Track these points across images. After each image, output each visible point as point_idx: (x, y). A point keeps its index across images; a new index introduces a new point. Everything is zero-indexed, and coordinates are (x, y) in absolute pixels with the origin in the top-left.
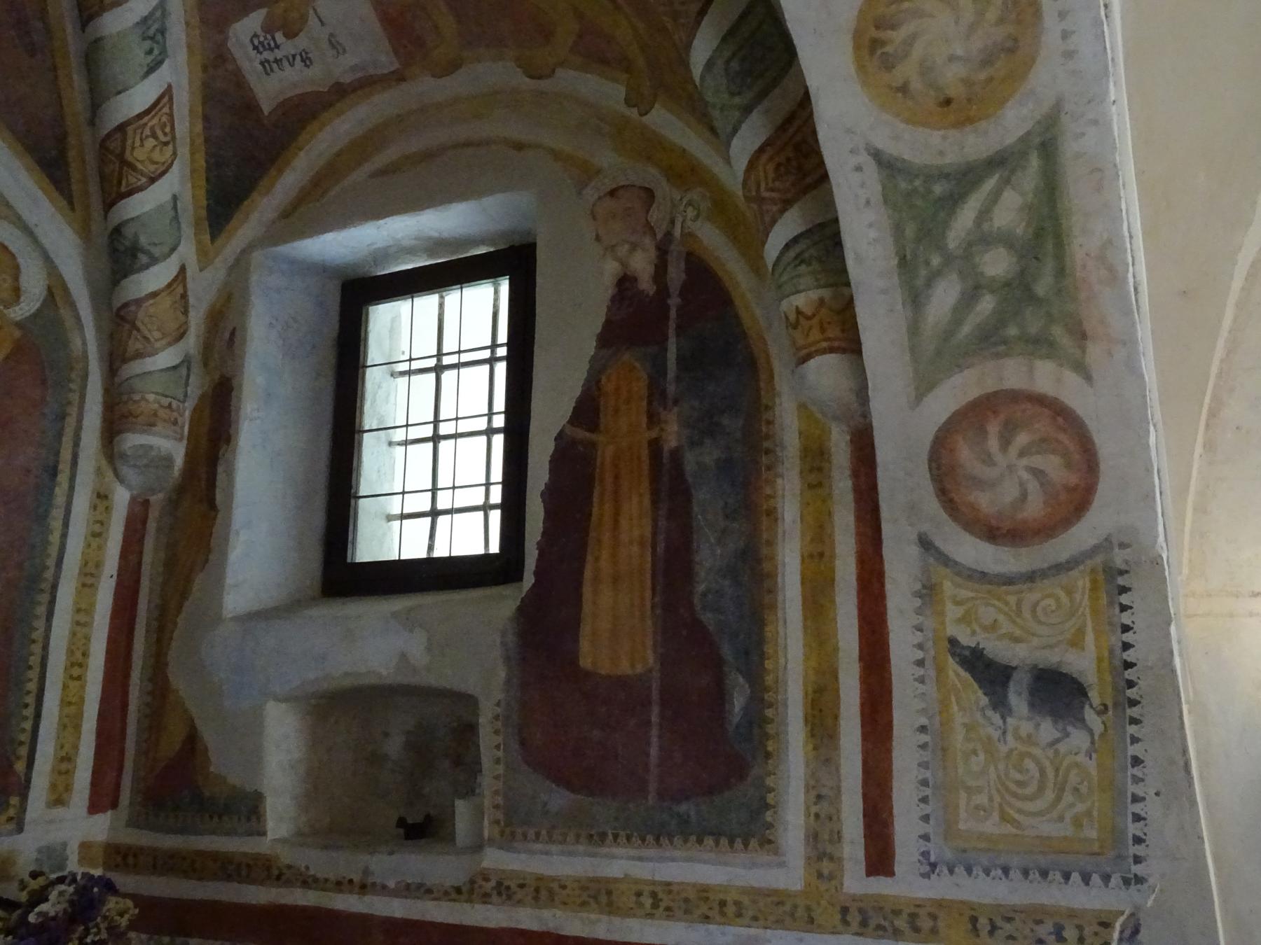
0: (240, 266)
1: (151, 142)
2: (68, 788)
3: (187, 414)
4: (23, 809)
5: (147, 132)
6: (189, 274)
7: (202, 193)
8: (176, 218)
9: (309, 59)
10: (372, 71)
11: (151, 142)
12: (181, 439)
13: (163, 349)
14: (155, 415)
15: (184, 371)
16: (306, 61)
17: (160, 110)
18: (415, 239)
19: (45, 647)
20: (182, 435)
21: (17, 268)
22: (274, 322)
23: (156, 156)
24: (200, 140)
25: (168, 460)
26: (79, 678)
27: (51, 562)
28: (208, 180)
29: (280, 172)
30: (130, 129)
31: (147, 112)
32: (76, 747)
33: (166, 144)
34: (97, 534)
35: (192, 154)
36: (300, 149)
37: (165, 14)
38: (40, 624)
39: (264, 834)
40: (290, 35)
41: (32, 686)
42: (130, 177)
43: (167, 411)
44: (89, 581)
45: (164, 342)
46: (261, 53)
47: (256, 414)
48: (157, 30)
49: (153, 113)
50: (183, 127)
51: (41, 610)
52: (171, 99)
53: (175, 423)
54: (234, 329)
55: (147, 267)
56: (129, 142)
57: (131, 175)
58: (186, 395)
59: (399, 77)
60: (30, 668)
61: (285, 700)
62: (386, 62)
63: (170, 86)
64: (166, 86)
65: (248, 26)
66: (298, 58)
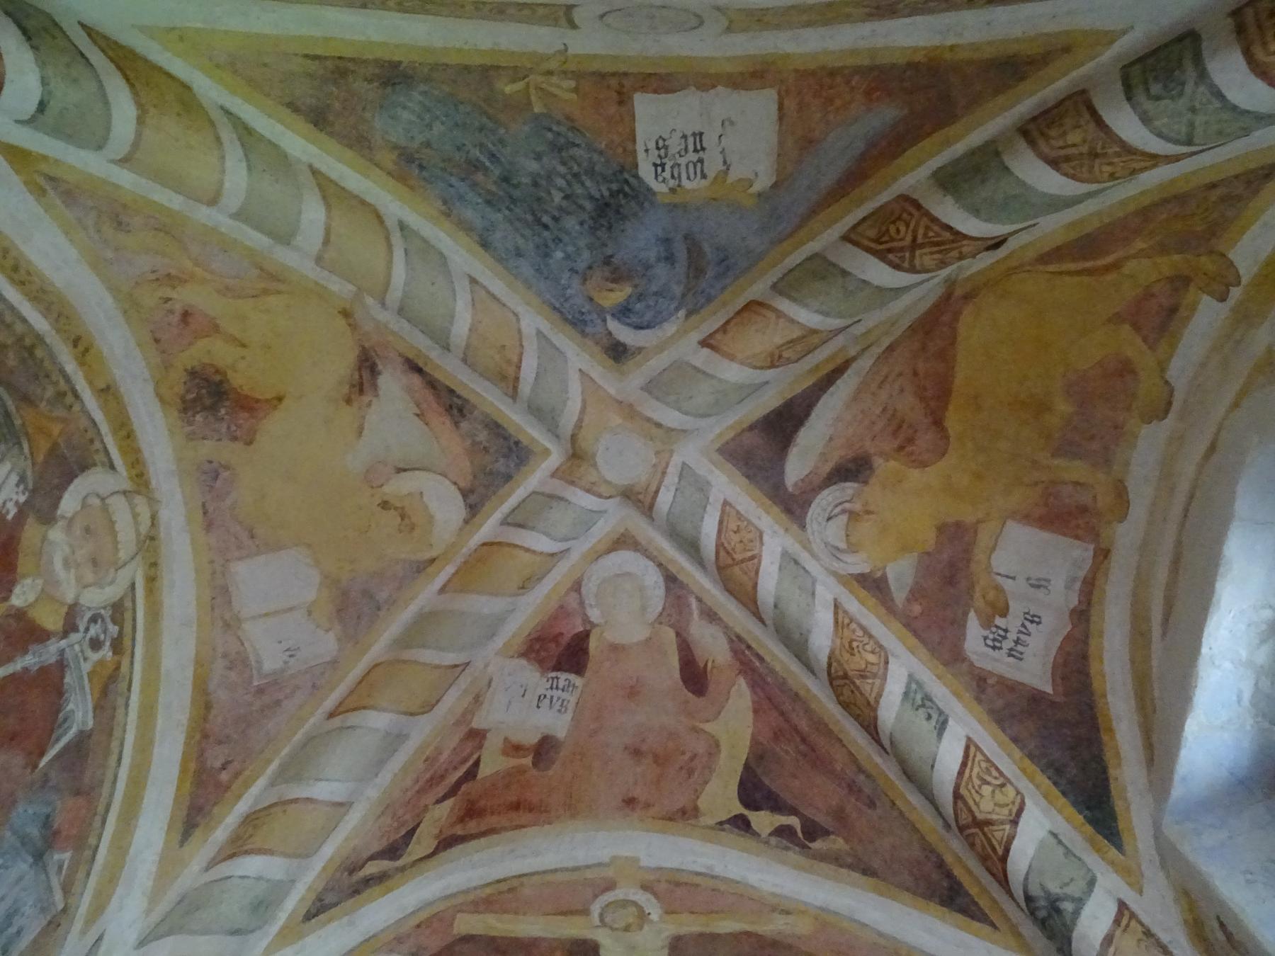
0: (1168, 856)
1: (987, 790)
5: (977, 782)
6: (1134, 906)
7: (1071, 810)
9: (1034, 616)
10: (1082, 574)
11: (987, 790)
16: (1034, 619)
17: (974, 760)
18: (1263, 641)
22: (1249, 876)
24: (1027, 762)
28: (1064, 794)
29: (1110, 730)
30: (963, 791)
31: (964, 764)
33: (1003, 785)
36: (1105, 696)
40: (1004, 613)
42: (995, 833)
46: (1000, 648)
49: (970, 764)
50: (1007, 765)
52: (978, 748)
54: (1218, 918)
55: (1077, 913)
56: (971, 803)
57: (996, 831)
59: (1103, 554)
62: (1082, 553)
65: (974, 637)
66: (1027, 623)
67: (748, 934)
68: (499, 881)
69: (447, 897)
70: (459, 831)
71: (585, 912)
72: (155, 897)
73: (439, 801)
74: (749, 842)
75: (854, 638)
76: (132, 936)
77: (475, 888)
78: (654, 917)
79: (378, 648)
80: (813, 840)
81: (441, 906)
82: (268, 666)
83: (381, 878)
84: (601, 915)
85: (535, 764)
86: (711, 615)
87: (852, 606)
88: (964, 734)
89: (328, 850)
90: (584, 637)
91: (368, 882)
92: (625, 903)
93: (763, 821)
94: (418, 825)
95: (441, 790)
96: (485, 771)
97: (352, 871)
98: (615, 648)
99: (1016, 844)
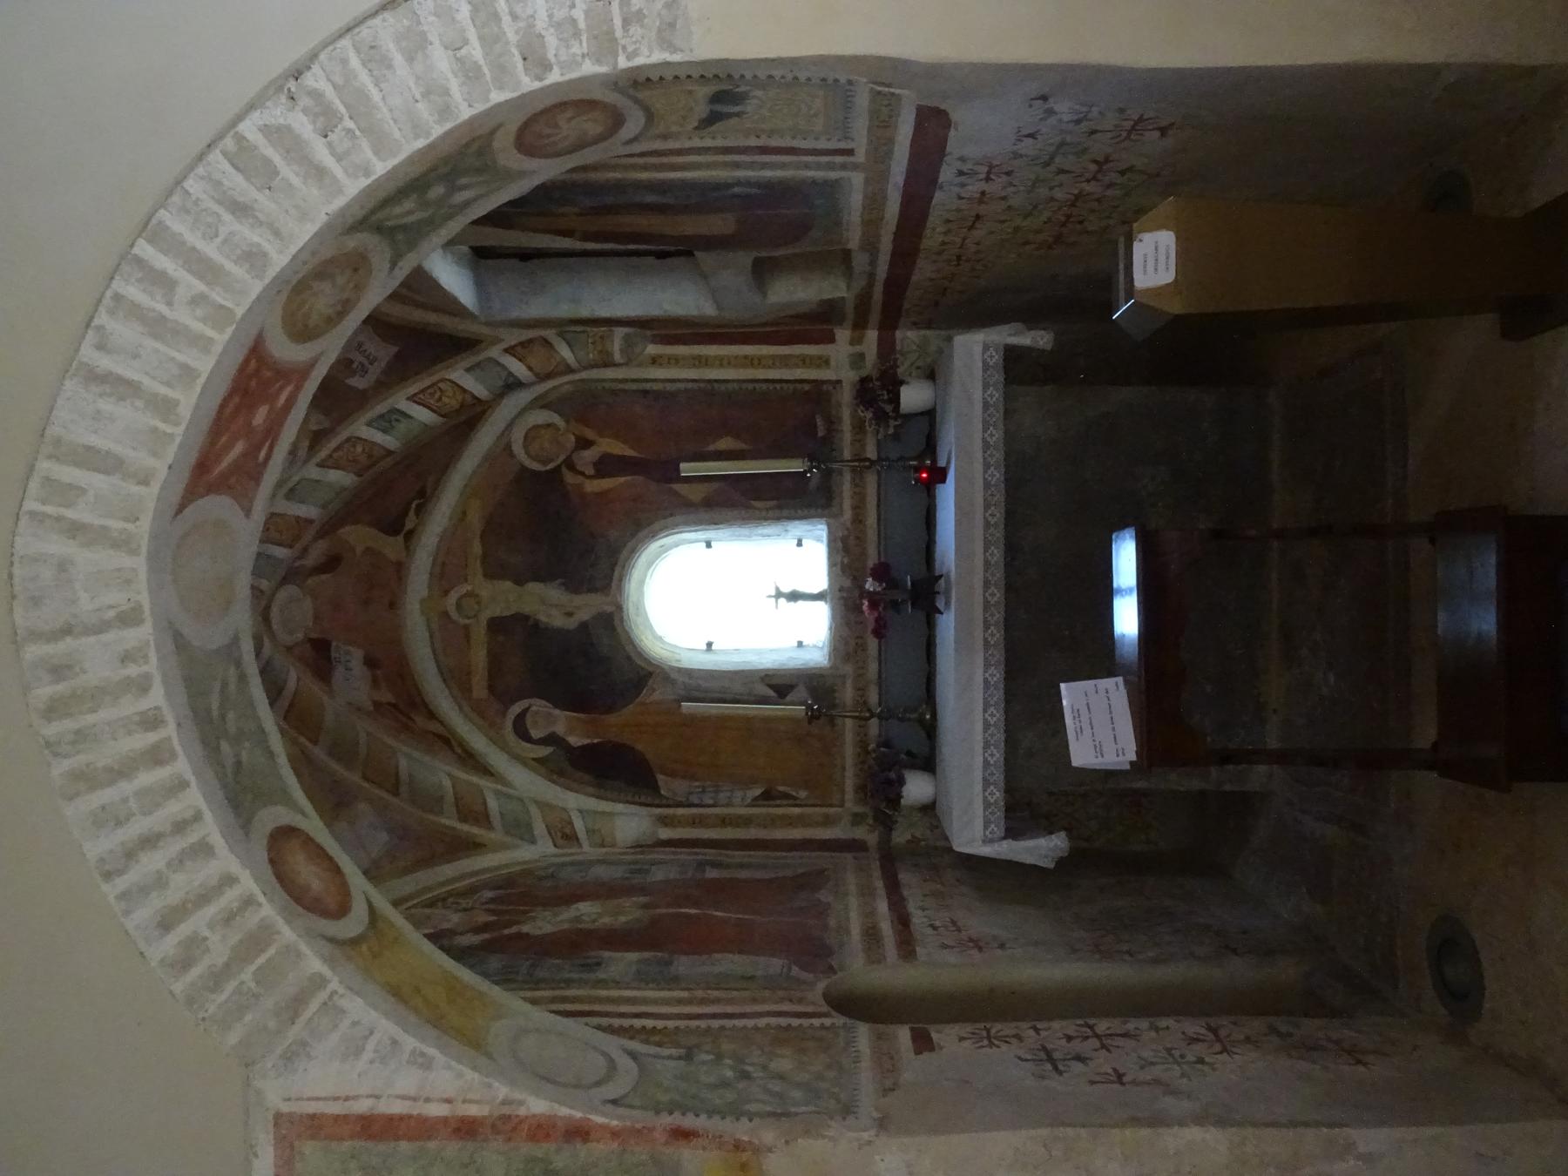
2: (820, 358)
3: (595, 329)
8: (478, 365)
14: (601, 352)
25: (627, 338)
27: (695, 386)
31: (429, 408)
34: (675, 361)
38: (730, 386)
39: (843, 298)
40: (352, 362)
41: (764, 386)
50: (427, 382)
51: (723, 387)
52: (415, 395)
53: (602, 337)
58: (584, 332)
61: (764, 294)
63: (408, 399)
64: (408, 402)
65: (358, 382)
66: (361, 349)
67: (481, 537)
71: (466, 628)
72: (516, 847)
75: (345, 458)
76: (533, 847)
78: (469, 588)
79: (354, 777)
81: (467, 709)
84: (469, 618)
86: (305, 550)
87: (323, 454)
90: (311, 640)
92: (459, 606)
93: (410, 523)
98: (317, 617)
99: (476, 394)
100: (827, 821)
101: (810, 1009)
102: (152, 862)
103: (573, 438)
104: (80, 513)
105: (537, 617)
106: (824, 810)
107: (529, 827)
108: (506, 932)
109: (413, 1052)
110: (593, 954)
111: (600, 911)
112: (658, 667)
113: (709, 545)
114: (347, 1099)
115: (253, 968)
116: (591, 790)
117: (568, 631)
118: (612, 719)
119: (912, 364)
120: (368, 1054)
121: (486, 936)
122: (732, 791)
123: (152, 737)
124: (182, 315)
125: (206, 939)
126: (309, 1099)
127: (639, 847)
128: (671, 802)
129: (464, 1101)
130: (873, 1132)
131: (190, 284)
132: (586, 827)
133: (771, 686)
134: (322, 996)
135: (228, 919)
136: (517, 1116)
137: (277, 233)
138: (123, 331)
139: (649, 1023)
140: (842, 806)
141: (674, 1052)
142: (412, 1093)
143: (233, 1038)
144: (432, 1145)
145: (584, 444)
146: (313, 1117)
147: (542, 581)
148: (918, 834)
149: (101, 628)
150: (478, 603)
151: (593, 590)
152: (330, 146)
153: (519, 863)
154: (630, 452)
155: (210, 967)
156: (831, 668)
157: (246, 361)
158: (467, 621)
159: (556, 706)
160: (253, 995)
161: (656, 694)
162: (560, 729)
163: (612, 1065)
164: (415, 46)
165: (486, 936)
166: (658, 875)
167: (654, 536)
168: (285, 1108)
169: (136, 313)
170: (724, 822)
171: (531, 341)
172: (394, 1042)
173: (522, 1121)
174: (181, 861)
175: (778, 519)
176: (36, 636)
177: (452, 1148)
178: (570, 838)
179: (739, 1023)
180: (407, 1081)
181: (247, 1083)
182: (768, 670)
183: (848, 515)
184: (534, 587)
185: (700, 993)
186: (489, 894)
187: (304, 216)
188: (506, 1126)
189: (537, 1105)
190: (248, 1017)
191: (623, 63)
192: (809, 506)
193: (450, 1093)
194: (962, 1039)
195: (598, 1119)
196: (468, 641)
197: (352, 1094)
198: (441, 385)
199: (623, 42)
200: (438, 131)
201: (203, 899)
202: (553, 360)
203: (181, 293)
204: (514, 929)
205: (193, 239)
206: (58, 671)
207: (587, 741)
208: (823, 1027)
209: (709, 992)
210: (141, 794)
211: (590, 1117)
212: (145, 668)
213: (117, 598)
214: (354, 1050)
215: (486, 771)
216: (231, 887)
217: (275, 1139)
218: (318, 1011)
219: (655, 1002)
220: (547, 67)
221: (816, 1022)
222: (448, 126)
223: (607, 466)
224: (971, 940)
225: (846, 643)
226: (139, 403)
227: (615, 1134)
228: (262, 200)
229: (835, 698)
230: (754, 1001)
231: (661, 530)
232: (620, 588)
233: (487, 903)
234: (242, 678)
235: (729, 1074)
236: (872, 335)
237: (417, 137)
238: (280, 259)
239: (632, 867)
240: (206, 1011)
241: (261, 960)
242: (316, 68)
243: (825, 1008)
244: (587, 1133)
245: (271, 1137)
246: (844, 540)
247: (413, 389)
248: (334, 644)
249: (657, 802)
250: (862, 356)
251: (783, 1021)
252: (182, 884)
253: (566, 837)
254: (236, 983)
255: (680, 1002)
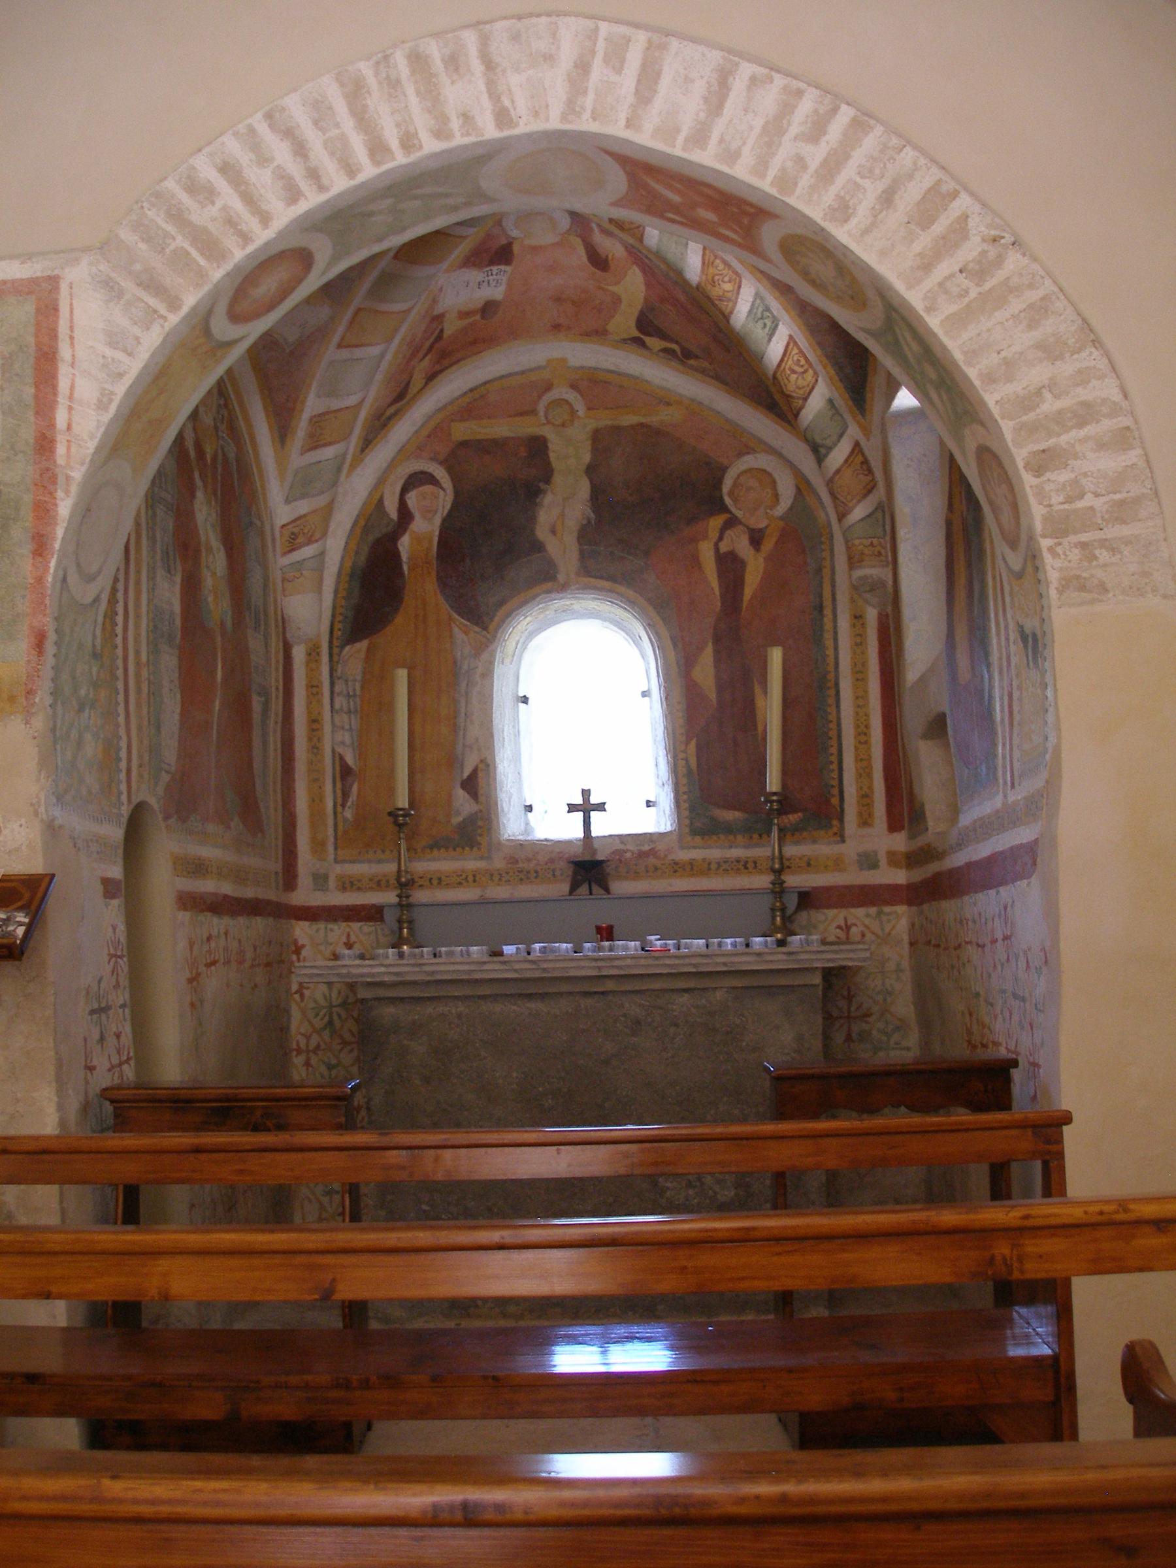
1: (793, 377)
2: (870, 815)
4: (842, 828)
11: (793, 377)
12: (887, 566)
13: (856, 505)
14: (862, 554)
15: (879, 515)
19: (839, 725)
20: (888, 562)
21: (774, 482)
23: (801, 382)
25: (883, 584)
26: (866, 742)
27: (831, 668)
28: (841, 380)
32: (871, 788)
33: (805, 372)
34: (859, 643)
35: (825, 368)
37: (762, 299)
38: (833, 710)
41: (834, 750)
43: (870, 548)
44: (860, 676)
45: (855, 501)
47: (907, 536)
48: (764, 311)
51: (831, 701)
52: (796, 343)
53: (880, 554)
60: (831, 738)
63: (791, 337)
64: (787, 338)
67: (642, 425)
68: (471, 390)
69: (440, 410)
70: (438, 367)
71: (533, 412)
73: (421, 360)
74: (645, 352)
75: (717, 272)
77: (457, 399)
78: (581, 413)
80: (688, 359)
82: (292, 339)
83: (395, 414)
85: (483, 318)
88: (788, 333)
89: (363, 415)
90: (510, 244)
91: (389, 418)
93: (654, 343)
94: (411, 377)
95: (421, 354)
96: (447, 333)
97: (379, 420)
98: (535, 249)
99: (803, 412)
100: (318, 846)
101: (134, 785)
102: (281, 152)
103: (762, 525)
104: (598, 71)
105: (549, 493)
106: (332, 839)
107: (303, 496)
108: (197, 475)
109: (112, 393)
110: (179, 568)
111: (218, 574)
112: (494, 637)
113: (645, 694)
114: (72, 338)
115: (187, 245)
116: (348, 564)
117: (533, 531)
118: (431, 586)
119: (866, 926)
120: (109, 352)
121: (192, 453)
122: (351, 729)
123: (394, 144)
124: (786, 149)
125: (213, 203)
126: (71, 304)
127: (284, 623)
128: (335, 658)
129: (68, 441)
130: (44, 817)
131: (816, 155)
132: (304, 560)
133: (475, 772)
134: (162, 309)
135: (231, 222)
136: (56, 490)
137: (866, 231)
138: (769, 99)
139: (120, 619)
140: (336, 861)
141: (98, 641)
142: (76, 395)
143: (126, 235)
144: (30, 416)
145: (756, 539)
146: (56, 310)
147: (592, 498)
148: (304, 953)
149: (495, 97)
150: (563, 425)
151: (583, 556)
152: (952, 275)
153: (263, 488)
154: (748, 592)
155: (188, 210)
156: (499, 843)
157: (751, 205)
158: (542, 413)
159: (444, 520)
160: (163, 249)
161: (462, 635)
162: (419, 525)
163: (90, 579)
164: (1051, 351)
165: (192, 453)
166: (254, 642)
167: (650, 626)
168: (64, 286)
169: (786, 109)
170: (314, 723)
171: (870, 471)
172: (121, 375)
173: (52, 494)
174: (282, 177)
175: (674, 770)
176: (484, 42)
177: (28, 434)
178: (293, 544)
179: (121, 709)
180: (87, 390)
181: (86, 249)
182: (495, 768)
183: (684, 855)
184: (584, 489)
185: (145, 673)
186: (232, 456)
187: (883, 253)
188: (47, 480)
189: (65, 508)
190: (143, 246)
191: (1045, 543)
192: (692, 809)
193: (76, 429)
194: (114, 928)
195: (53, 563)
196: (516, 415)
197: (76, 341)
198: (811, 372)
199: (1065, 541)
200: (972, 373)
201: (249, 199)
202: (849, 497)
203: (807, 149)
204: (199, 482)
205: (858, 157)
206: (454, 62)
207: (404, 557)
208: (120, 793)
209: (147, 682)
210: (343, 139)
211: (55, 556)
212: (458, 134)
213: (521, 106)
214: (114, 339)
215: (367, 444)
216: (260, 222)
217: (37, 278)
218: (149, 306)
219: (137, 627)
220: (1038, 471)
221: (123, 787)
222: (977, 383)
223: (731, 566)
224: (198, 974)
225: (529, 860)
226: (702, 115)
227: (40, 580)
228: (895, 218)
229: (463, 848)
230: (140, 728)
231: (657, 634)
232: (585, 588)
233: (223, 451)
234: (455, 208)
235: (83, 692)
236: (900, 877)
237: (965, 353)
238: (843, 234)
239: (262, 610)
240: (149, 210)
241: (195, 254)
242: (1026, 261)
243: (135, 801)
244: (41, 555)
245: (39, 274)
246: (652, 852)
247: (803, 342)
248: (508, 268)
249: (336, 643)
250: (874, 865)
251: (123, 754)
252: (261, 178)
253: (294, 536)
254: (173, 233)
255: (137, 653)
